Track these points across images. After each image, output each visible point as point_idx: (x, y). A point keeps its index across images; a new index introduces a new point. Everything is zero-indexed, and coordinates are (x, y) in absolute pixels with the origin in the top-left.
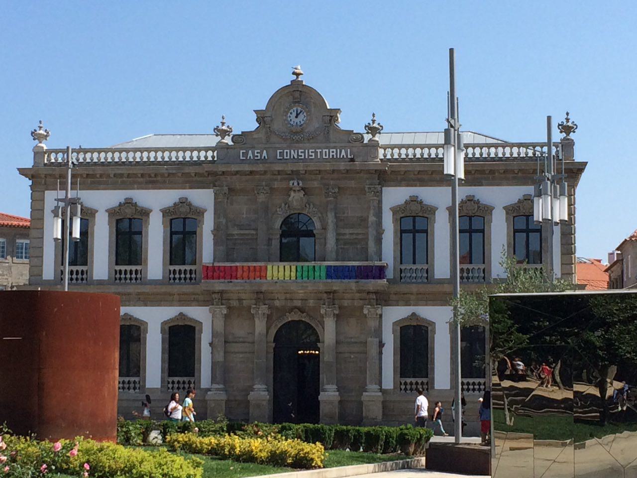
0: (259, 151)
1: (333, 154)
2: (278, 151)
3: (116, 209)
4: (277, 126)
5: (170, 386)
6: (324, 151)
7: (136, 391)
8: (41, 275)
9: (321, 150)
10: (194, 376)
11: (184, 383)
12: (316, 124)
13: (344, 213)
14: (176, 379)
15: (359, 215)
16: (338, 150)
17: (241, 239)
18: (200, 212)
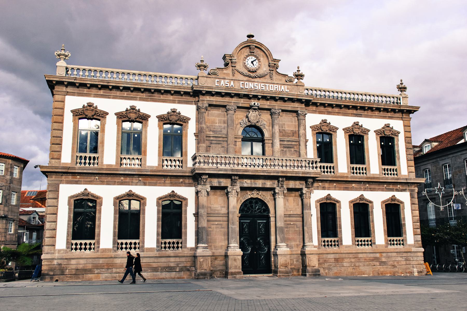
0: (228, 81)
1: (276, 88)
2: (241, 83)
3: (123, 113)
4: (239, 67)
5: (163, 245)
6: (271, 85)
7: (136, 250)
8: (59, 158)
9: (268, 85)
10: (181, 238)
11: (173, 243)
12: (265, 69)
13: (282, 128)
14: (168, 241)
15: (292, 129)
16: (280, 86)
17: (215, 140)
18: (186, 120)
